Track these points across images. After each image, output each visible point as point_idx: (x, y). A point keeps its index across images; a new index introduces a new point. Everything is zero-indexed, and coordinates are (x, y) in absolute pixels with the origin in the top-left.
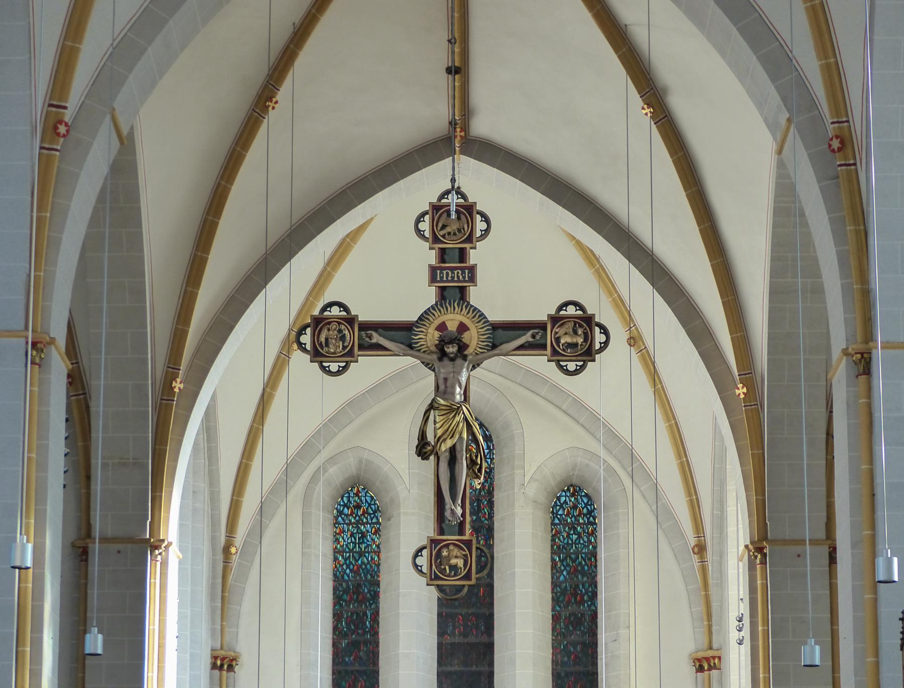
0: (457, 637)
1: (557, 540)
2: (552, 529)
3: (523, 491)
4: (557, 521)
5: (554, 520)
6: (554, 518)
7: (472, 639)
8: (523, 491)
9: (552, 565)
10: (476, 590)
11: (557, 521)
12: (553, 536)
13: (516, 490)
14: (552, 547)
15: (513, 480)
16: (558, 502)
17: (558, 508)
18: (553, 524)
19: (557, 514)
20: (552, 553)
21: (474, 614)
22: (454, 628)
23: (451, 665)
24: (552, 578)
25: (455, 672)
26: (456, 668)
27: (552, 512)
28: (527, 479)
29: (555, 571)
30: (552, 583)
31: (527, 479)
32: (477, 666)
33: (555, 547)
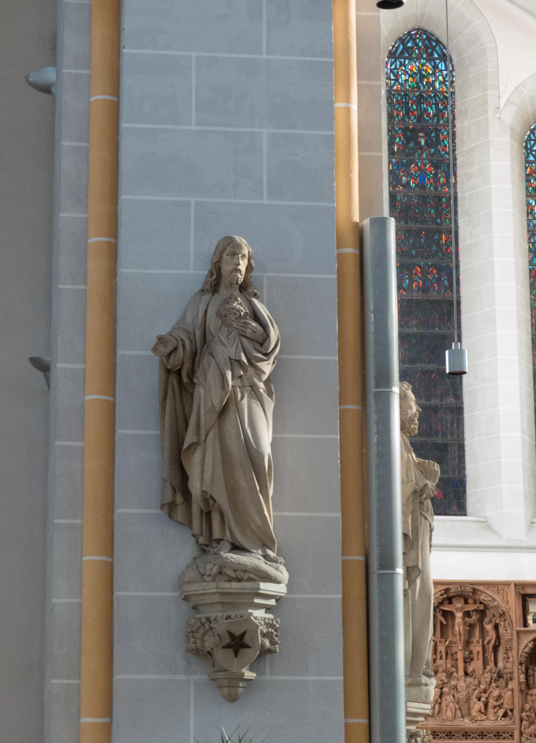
0: (415, 293)
1: (532, 181)
2: (526, 168)
3: (498, 115)
4: (531, 158)
5: (527, 157)
6: (528, 155)
7: (433, 295)
8: (498, 115)
9: (528, 210)
10: (437, 237)
11: (531, 158)
12: (527, 175)
13: (490, 115)
14: (527, 188)
15: (486, 103)
16: (532, 136)
17: (532, 142)
18: (527, 162)
19: (531, 150)
20: (527, 196)
21: (434, 266)
22: (411, 281)
23: (408, 327)
24: (529, 225)
25: (415, 335)
26: (415, 330)
27: (526, 148)
28: (503, 101)
29: (531, 217)
30: (529, 231)
31: (503, 101)
32: (440, 328)
33: (530, 189)
